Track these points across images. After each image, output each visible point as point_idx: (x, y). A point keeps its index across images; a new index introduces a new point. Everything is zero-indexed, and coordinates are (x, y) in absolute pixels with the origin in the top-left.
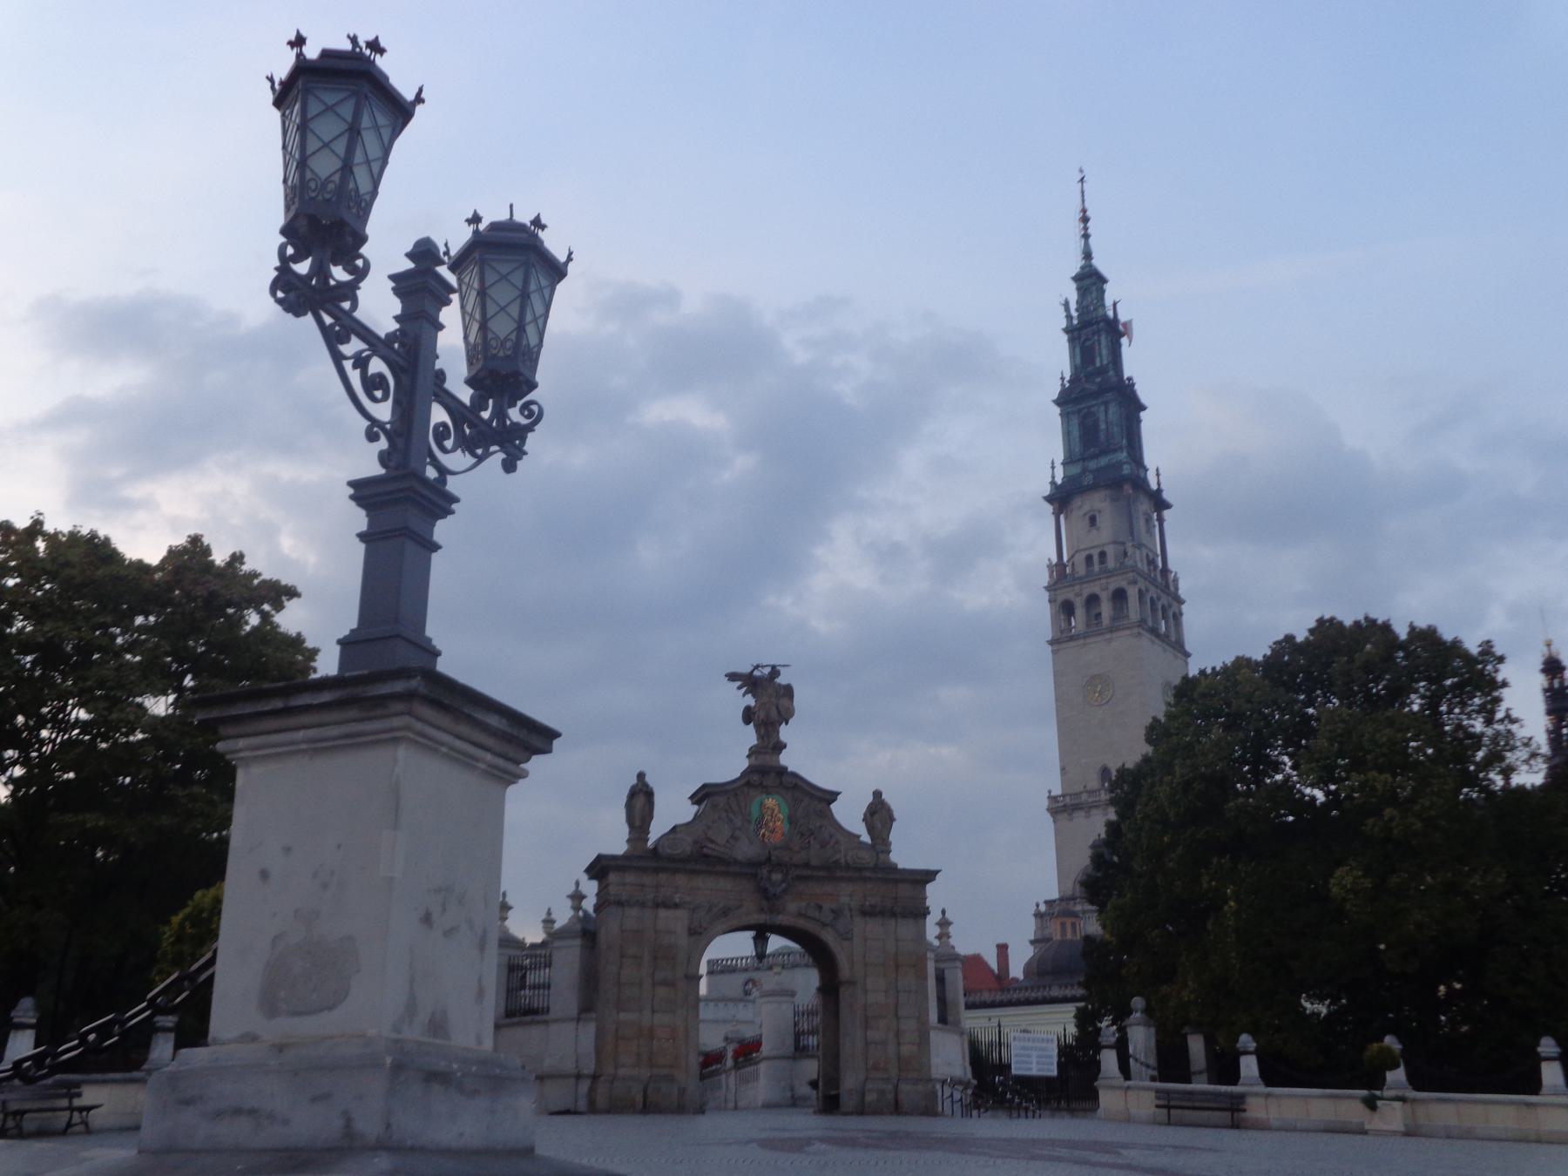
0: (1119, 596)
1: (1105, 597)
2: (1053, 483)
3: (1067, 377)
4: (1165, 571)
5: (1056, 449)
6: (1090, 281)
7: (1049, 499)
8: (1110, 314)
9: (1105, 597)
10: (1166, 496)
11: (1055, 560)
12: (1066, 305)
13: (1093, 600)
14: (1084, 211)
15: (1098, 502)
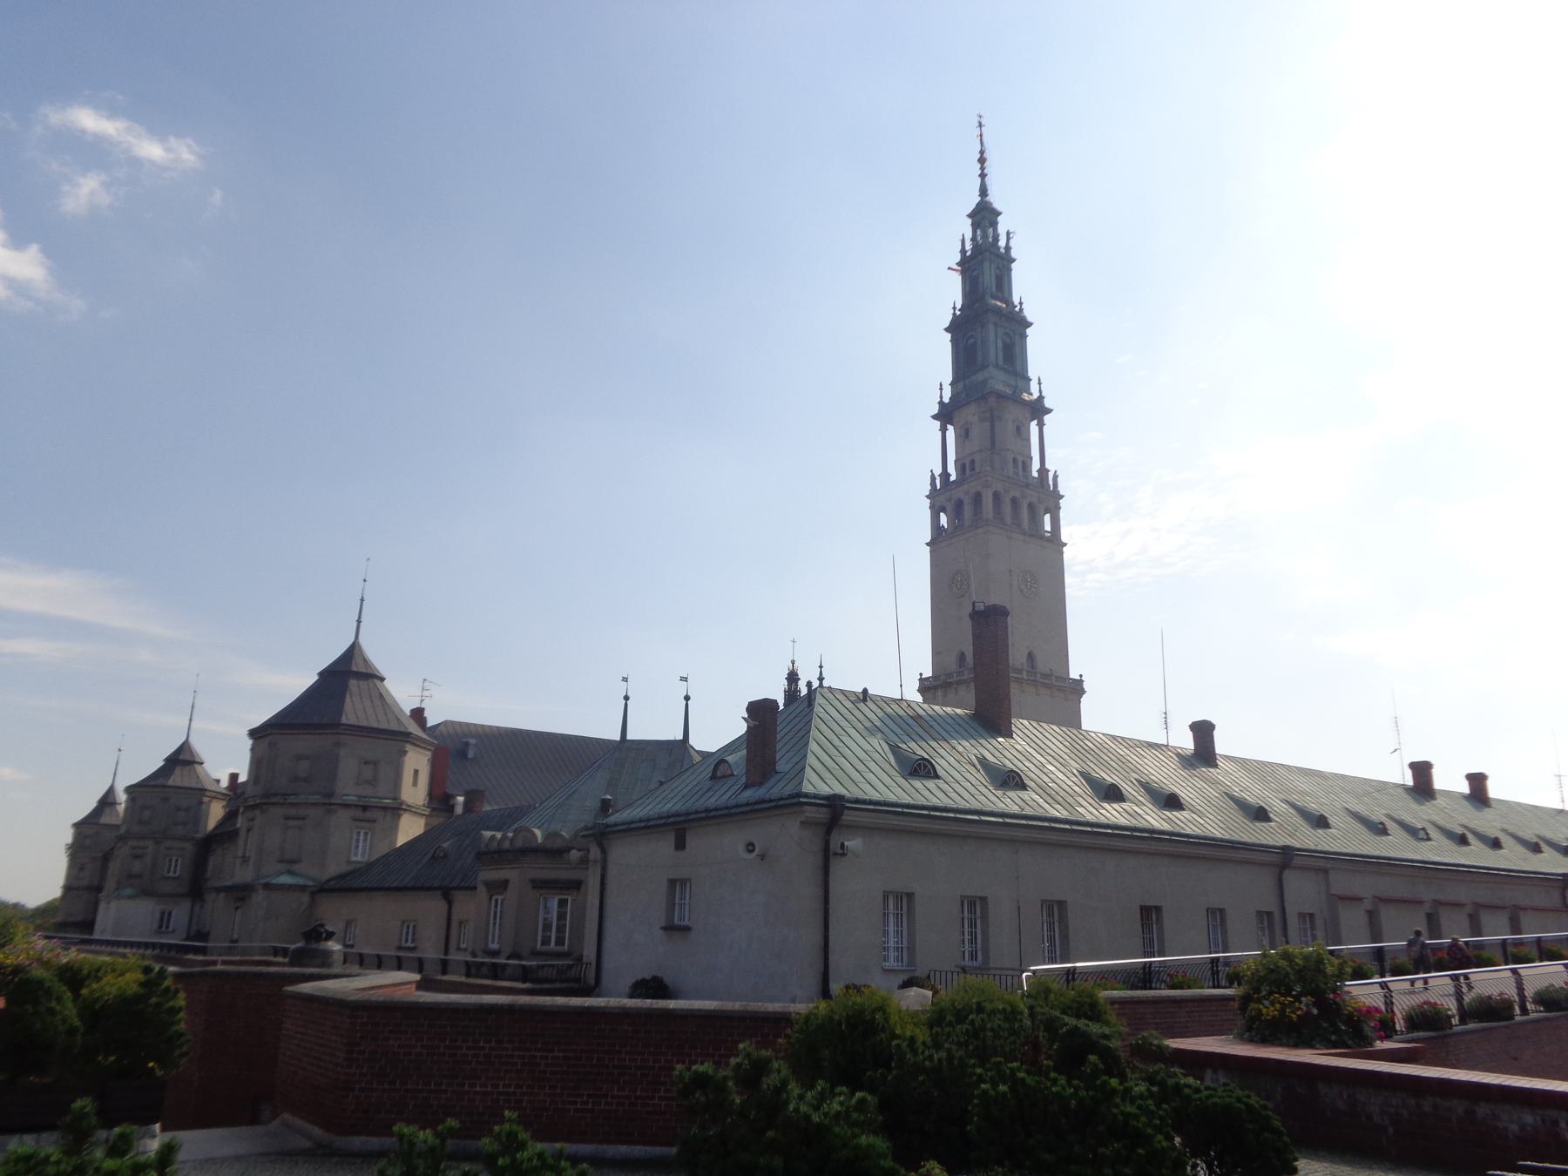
0: (977, 498)
1: (967, 501)
2: (941, 403)
3: (959, 306)
4: (1043, 470)
5: (946, 374)
6: (984, 216)
7: (935, 417)
8: (1002, 243)
9: (967, 501)
10: (1047, 403)
11: (938, 471)
12: (963, 241)
13: (959, 505)
14: (982, 152)
15: (970, 414)
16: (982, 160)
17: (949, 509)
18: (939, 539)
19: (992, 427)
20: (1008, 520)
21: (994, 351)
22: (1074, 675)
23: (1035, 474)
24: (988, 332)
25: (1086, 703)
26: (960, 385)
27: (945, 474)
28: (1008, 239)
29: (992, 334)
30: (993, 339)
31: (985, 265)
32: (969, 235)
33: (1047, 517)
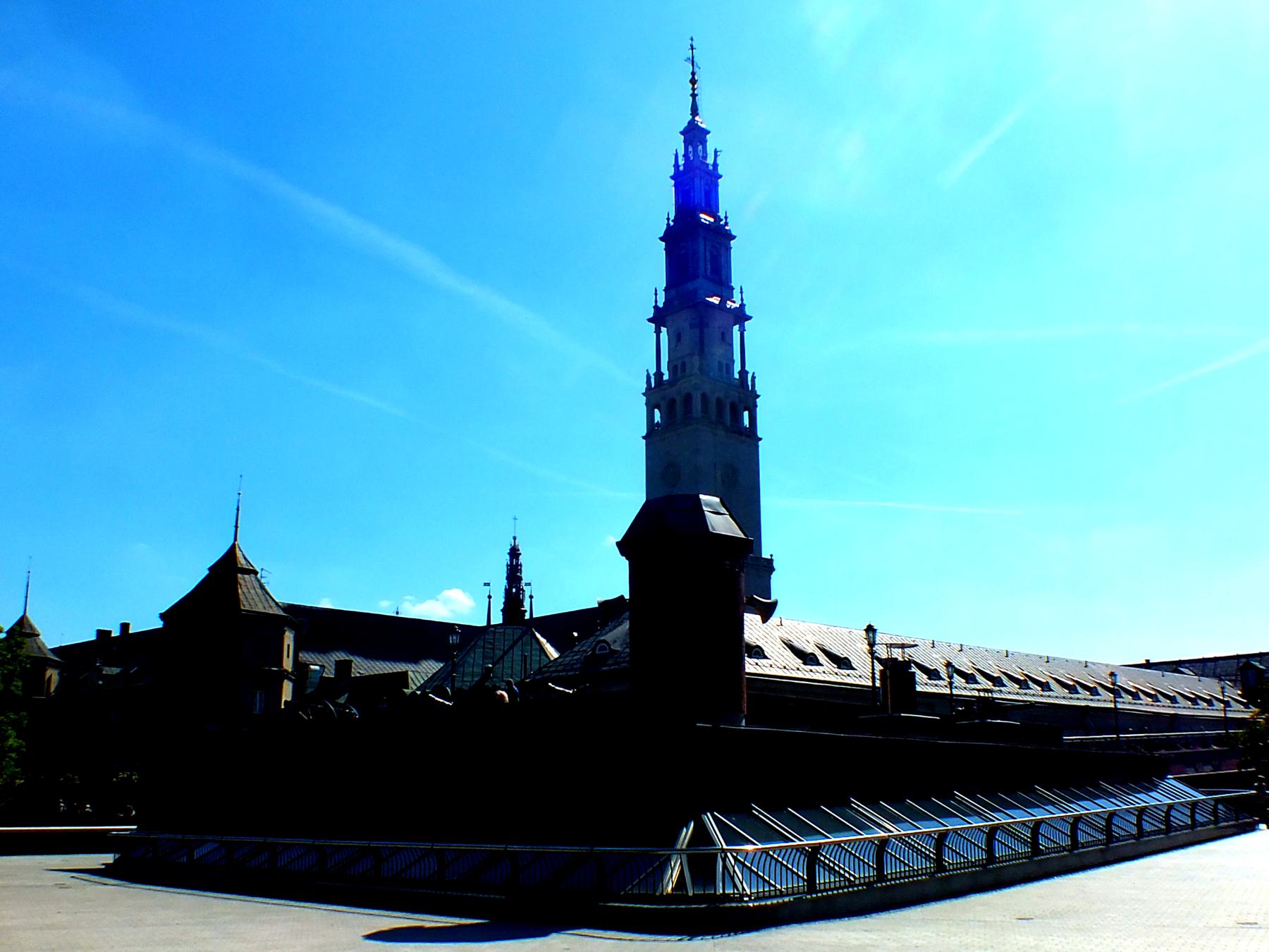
2: (656, 307)
3: (672, 217)
4: (743, 372)
6: (694, 135)
8: (710, 160)
11: (653, 370)
13: (672, 402)
14: (693, 74)
16: (693, 81)
17: (664, 404)
18: (652, 434)
19: (702, 333)
20: (714, 418)
21: (704, 266)
22: (765, 555)
23: (737, 376)
24: (697, 248)
25: (775, 578)
26: (673, 292)
27: (659, 374)
28: (716, 156)
29: (702, 248)
30: (702, 248)
31: (695, 183)
32: (681, 152)
33: (746, 414)
